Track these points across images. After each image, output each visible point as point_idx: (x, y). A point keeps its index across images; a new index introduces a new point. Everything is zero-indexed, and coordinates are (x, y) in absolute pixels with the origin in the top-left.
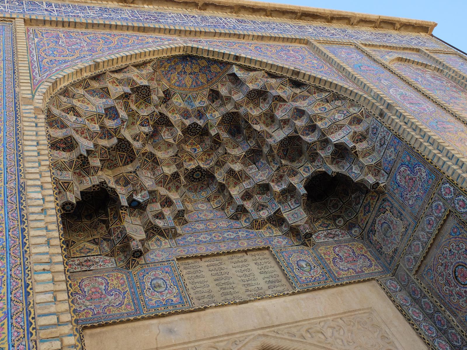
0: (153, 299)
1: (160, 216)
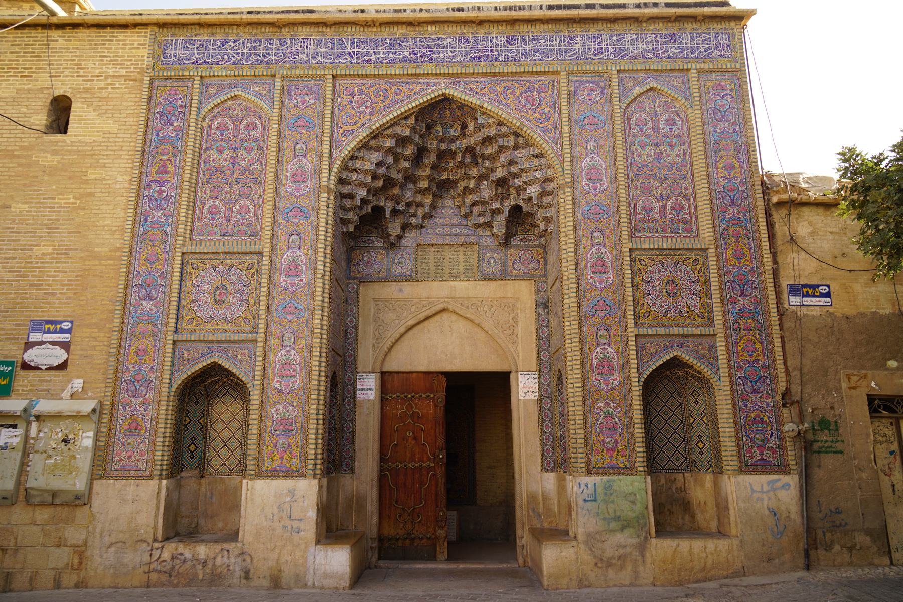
0: (397, 271)
1: (414, 215)
